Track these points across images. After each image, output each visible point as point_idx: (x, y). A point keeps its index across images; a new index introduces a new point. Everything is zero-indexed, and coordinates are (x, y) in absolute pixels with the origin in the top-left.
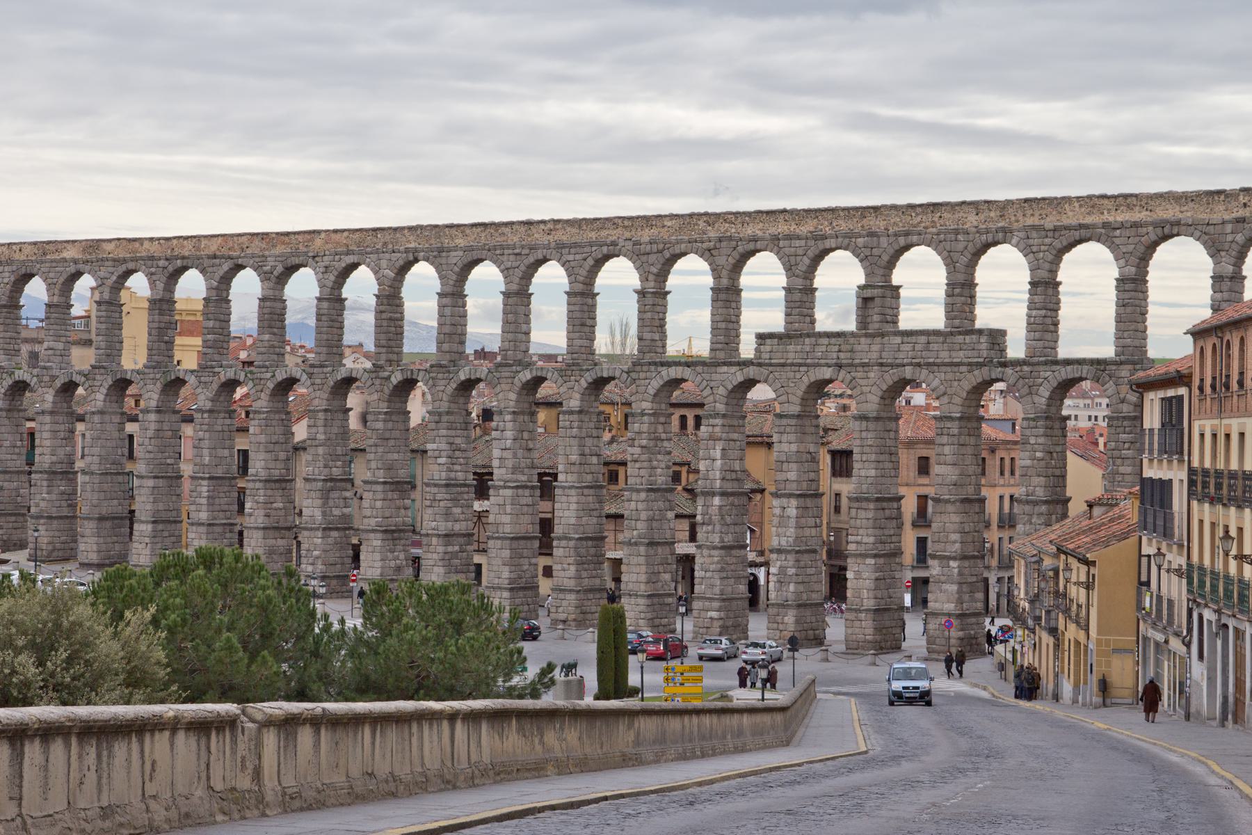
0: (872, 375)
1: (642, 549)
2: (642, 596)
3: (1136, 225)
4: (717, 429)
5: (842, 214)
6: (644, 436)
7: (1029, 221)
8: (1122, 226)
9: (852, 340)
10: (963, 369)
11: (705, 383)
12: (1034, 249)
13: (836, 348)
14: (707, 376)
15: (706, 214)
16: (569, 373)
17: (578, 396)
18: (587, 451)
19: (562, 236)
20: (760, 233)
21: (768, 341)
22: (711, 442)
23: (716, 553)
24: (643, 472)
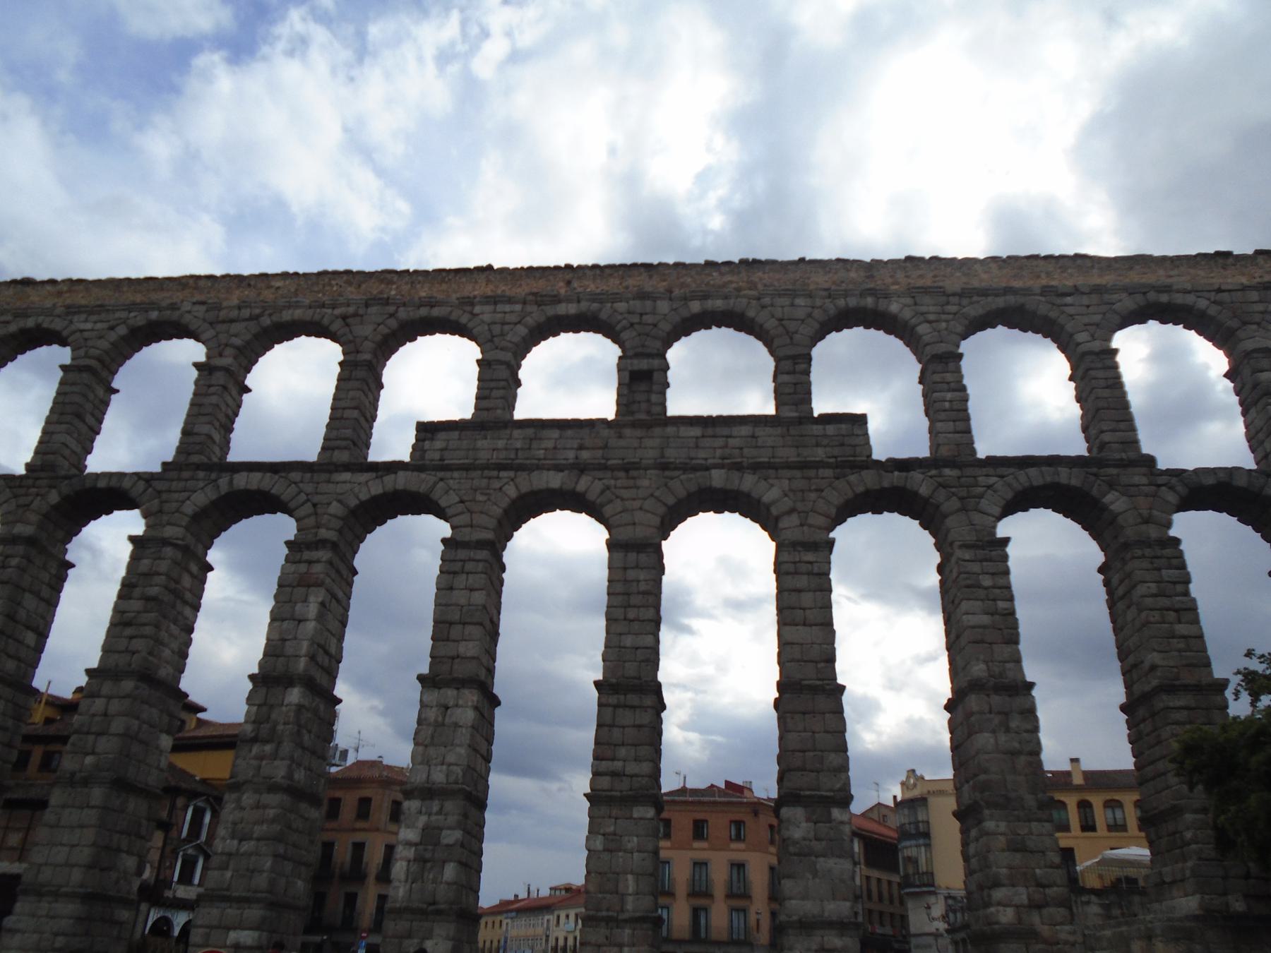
0: (646, 483)
1: (97, 794)
2: (71, 896)
3: (1098, 290)
4: (317, 568)
5: (588, 272)
6: (158, 579)
7: (920, 283)
8: (1076, 291)
9: (606, 432)
10: (828, 472)
11: (303, 497)
12: (931, 317)
13: (575, 444)
14: (309, 488)
15: (348, 272)
16: (30, 482)
17: (34, 518)
18: (22, 614)
19: (80, 299)
20: (440, 297)
21: (442, 435)
22: (303, 590)
23: (273, 799)
24: (138, 644)
